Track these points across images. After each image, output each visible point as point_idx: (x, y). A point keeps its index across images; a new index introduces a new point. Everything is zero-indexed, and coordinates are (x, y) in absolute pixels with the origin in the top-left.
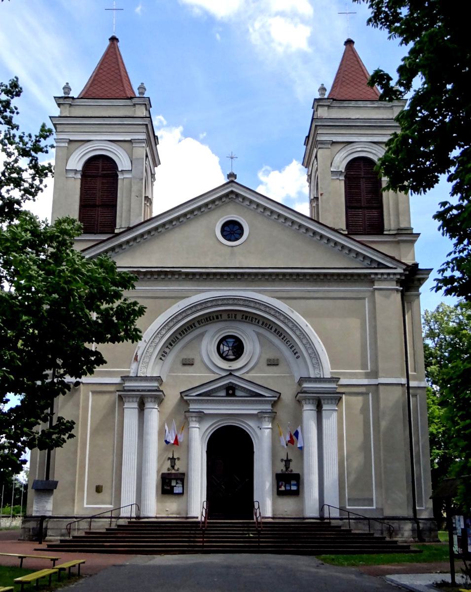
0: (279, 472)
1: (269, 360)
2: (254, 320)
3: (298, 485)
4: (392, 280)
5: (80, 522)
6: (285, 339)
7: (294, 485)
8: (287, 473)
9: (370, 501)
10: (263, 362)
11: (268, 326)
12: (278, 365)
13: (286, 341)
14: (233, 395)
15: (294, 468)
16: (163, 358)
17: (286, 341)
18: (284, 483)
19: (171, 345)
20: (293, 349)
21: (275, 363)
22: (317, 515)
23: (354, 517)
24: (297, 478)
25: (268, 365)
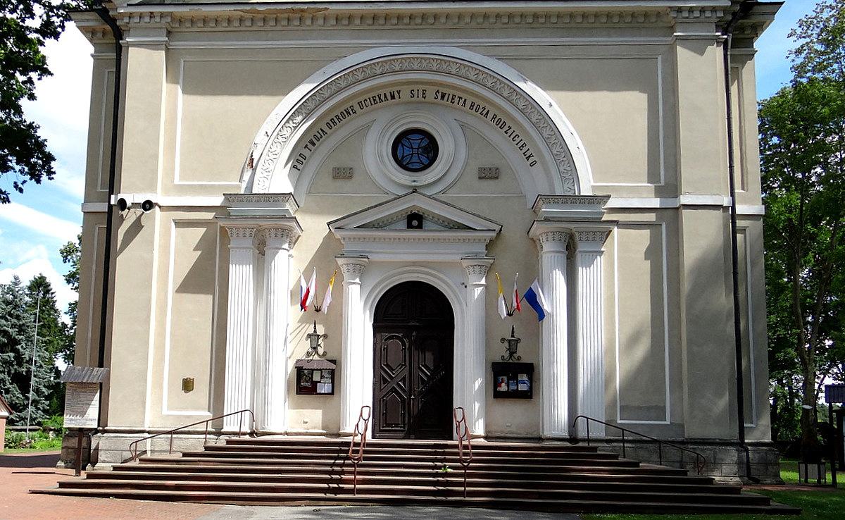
0: (498, 360)
1: (481, 170)
2: (456, 100)
3: (531, 380)
4: (707, 21)
5: (155, 439)
6: (510, 132)
7: (523, 382)
8: (511, 361)
9: (660, 412)
10: (473, 173)
11: (480, 110)
12: (497, 178)
13: (512, 136)
14: (420, 227)
15: (524, 354)
16: (299, 166)
17: (512, 136)
18: (505, 378)
19: (314, 144)
20: (525, 149)
21: (493, 174)
22: (565, 434)
23: (631, 438)
24: (530, 370)
25: (480, 178)
